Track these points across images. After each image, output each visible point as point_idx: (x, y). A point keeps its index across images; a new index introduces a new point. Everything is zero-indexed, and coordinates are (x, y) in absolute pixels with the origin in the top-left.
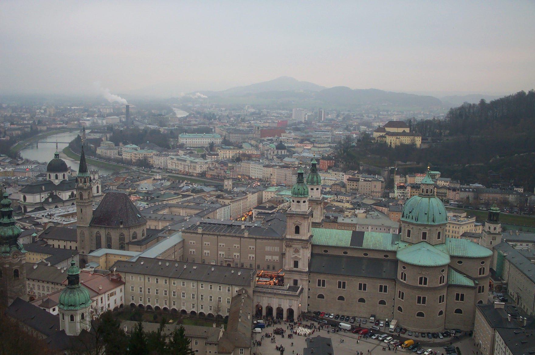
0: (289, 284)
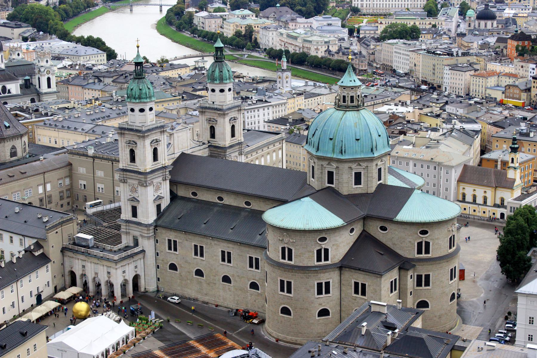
0: (126, 241)
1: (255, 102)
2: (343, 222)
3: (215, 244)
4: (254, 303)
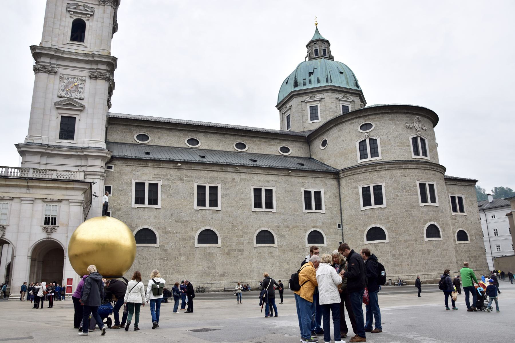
3: (241, 179)
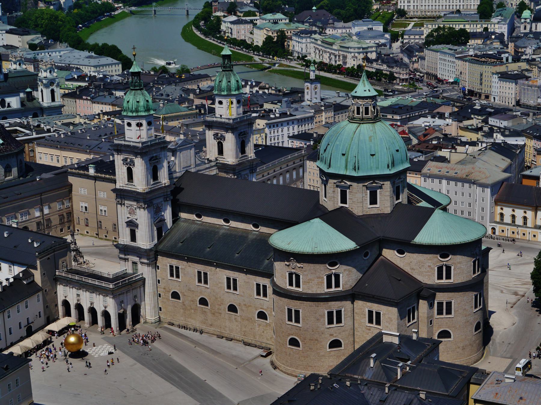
1: (277, 115)
2: (356, 245)
4: (263, 334)
